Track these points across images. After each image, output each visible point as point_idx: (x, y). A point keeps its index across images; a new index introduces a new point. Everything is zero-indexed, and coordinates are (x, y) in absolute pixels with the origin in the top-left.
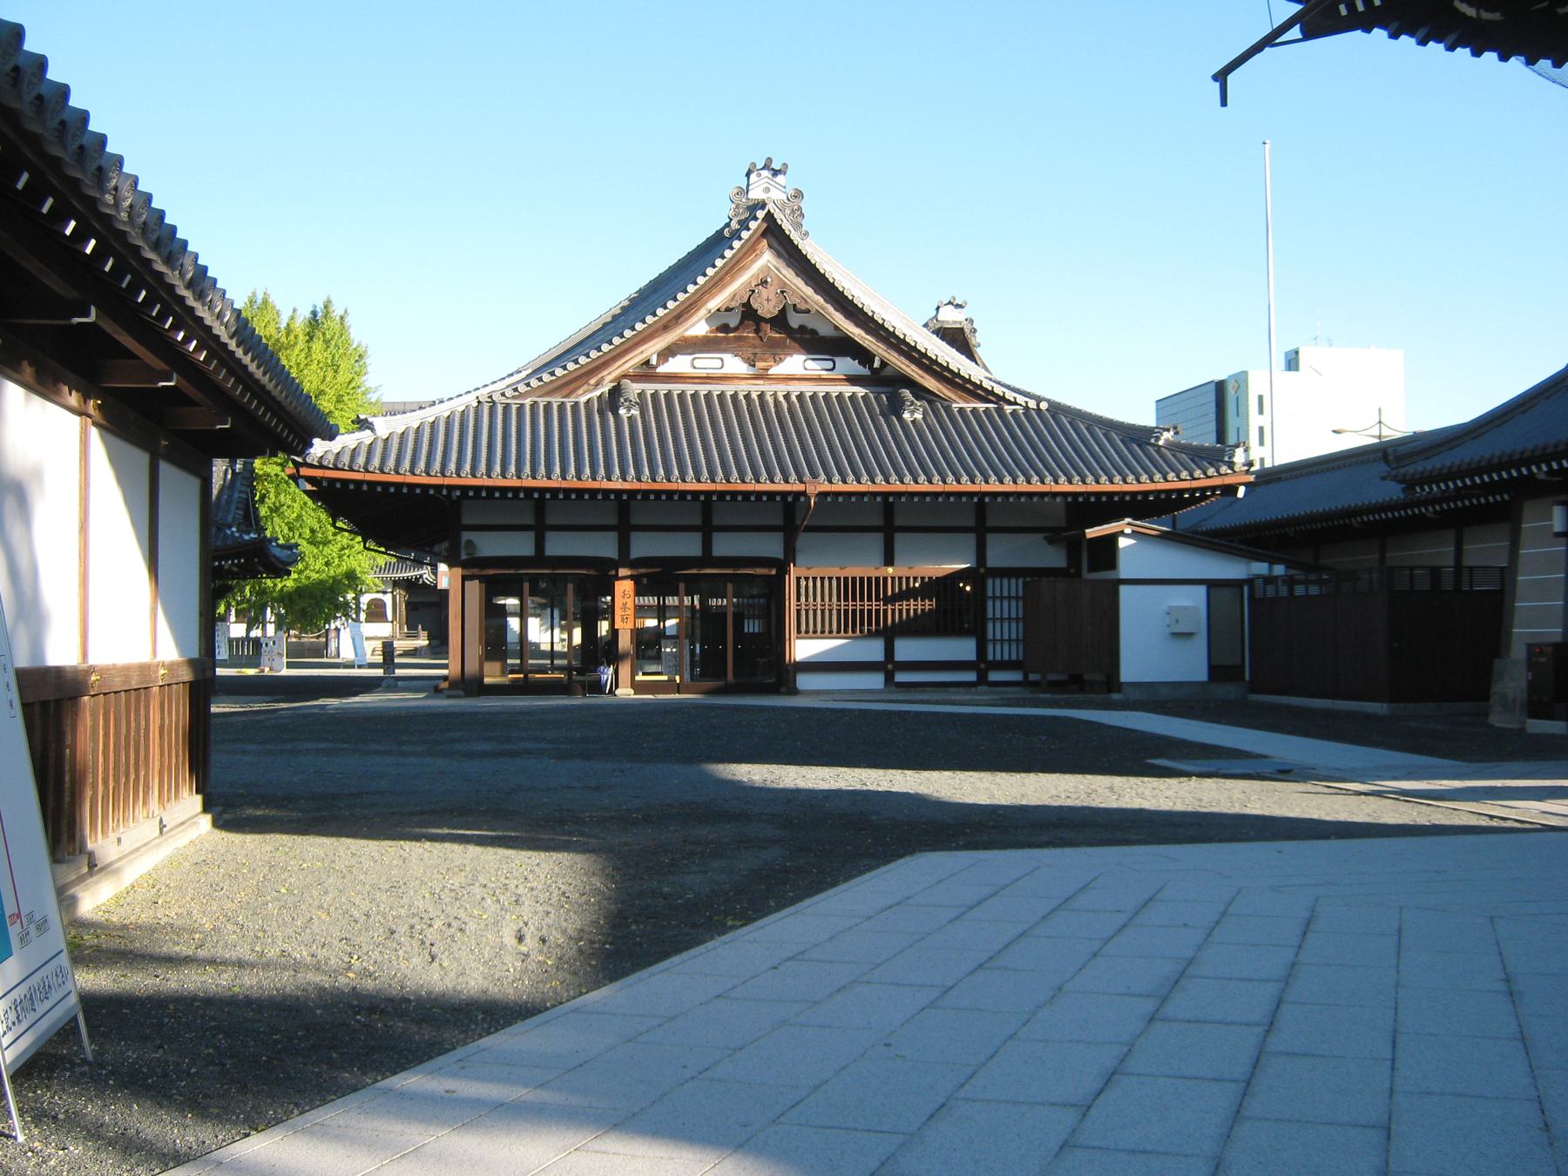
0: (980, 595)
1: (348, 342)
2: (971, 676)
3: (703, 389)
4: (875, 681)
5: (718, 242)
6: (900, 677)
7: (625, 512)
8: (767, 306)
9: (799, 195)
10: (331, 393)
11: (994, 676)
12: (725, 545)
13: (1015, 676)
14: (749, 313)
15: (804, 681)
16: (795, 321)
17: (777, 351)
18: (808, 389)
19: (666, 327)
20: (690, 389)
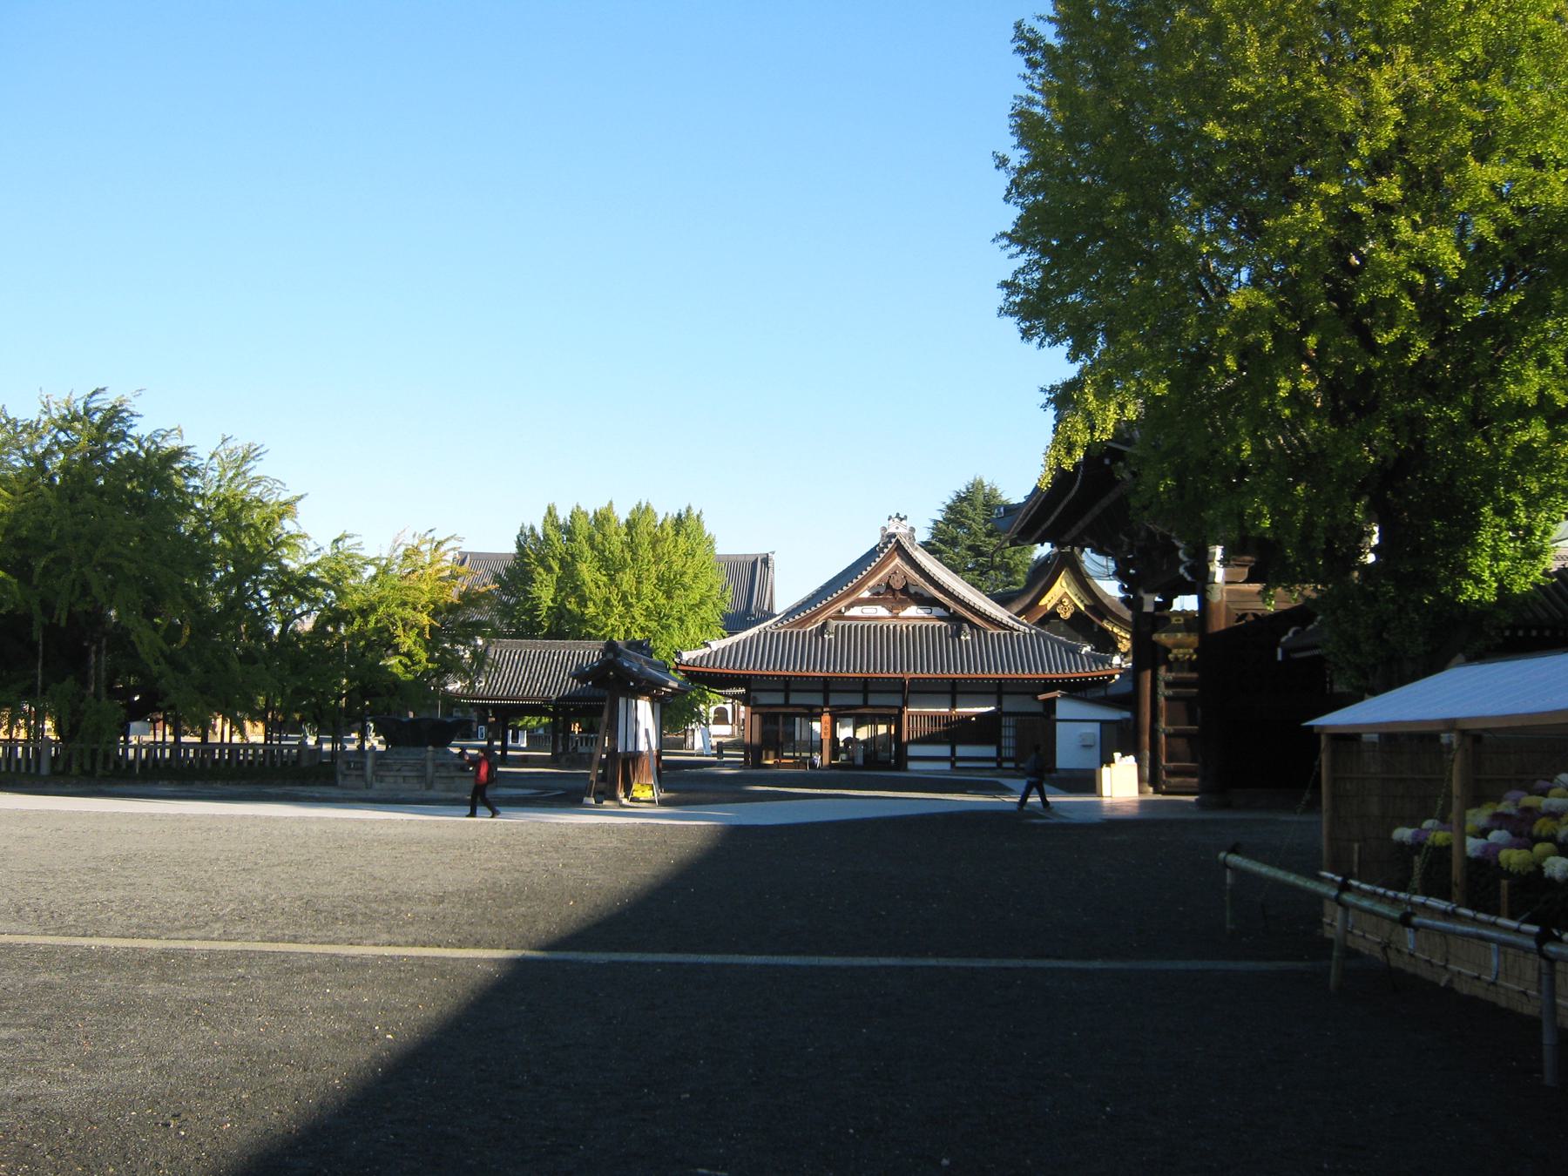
0: (1000, 727)
1: (701, 534)
2: (994, 765)
3: (867, 623)
4: (946, 766)
5: (873, 553)
6: (958, 764)
7: (826, 686)
8: (898, 585)
9: (913, 530)
10: (690, 571)
11: (1005, 765)
12: (874, 699)
13: (1012, 765)
14: (888, 586)
15: (912, 765)
16: (912, 590)
17: (904, 605)
18: (918, 623)
19: (848, 594)
20: (860, 623)
